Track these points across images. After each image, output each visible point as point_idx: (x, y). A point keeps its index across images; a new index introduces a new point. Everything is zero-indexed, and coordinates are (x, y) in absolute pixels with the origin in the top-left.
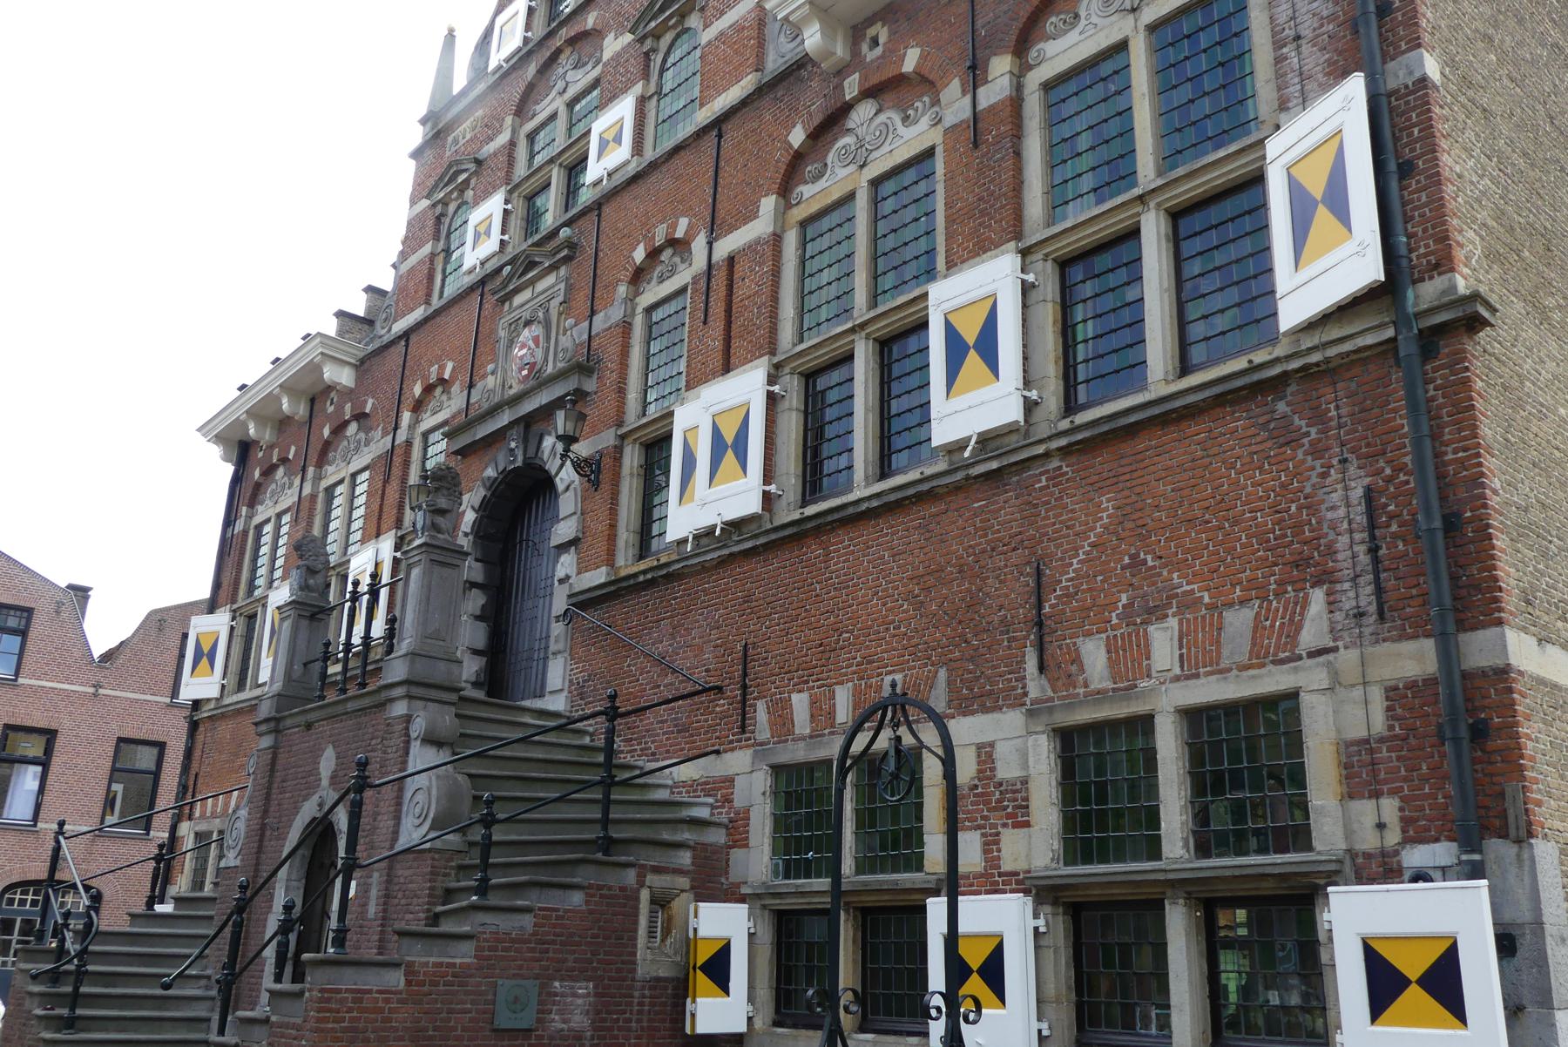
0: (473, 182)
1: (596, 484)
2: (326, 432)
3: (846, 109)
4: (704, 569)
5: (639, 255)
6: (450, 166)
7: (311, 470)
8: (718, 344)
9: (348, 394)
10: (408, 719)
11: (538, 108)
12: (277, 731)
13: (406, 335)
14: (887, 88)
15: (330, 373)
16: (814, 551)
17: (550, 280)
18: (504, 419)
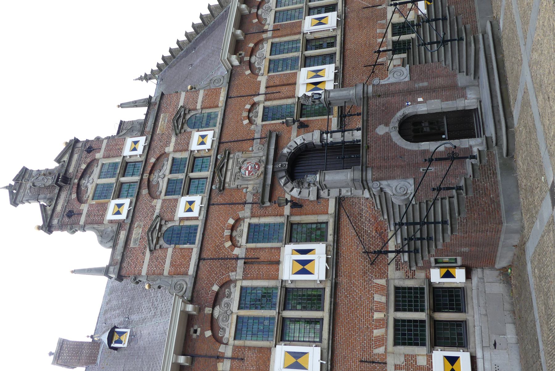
0: (163, 222)
1: (307, 126)
2: (208, 333)
3: (250, 61)
4: (343, 82)
5: (246, 122)
6: (148, 234)
7: (222, 349)
8: (287, 87)
9: (200, 310)
10: (374, 85)
11: (160, 190)
12: (366, 167)
13: (200, 259)
14: (252, 52)
15: (190, 308)
16: (348, 53)
17: (231, 161)
18: (270, 167)
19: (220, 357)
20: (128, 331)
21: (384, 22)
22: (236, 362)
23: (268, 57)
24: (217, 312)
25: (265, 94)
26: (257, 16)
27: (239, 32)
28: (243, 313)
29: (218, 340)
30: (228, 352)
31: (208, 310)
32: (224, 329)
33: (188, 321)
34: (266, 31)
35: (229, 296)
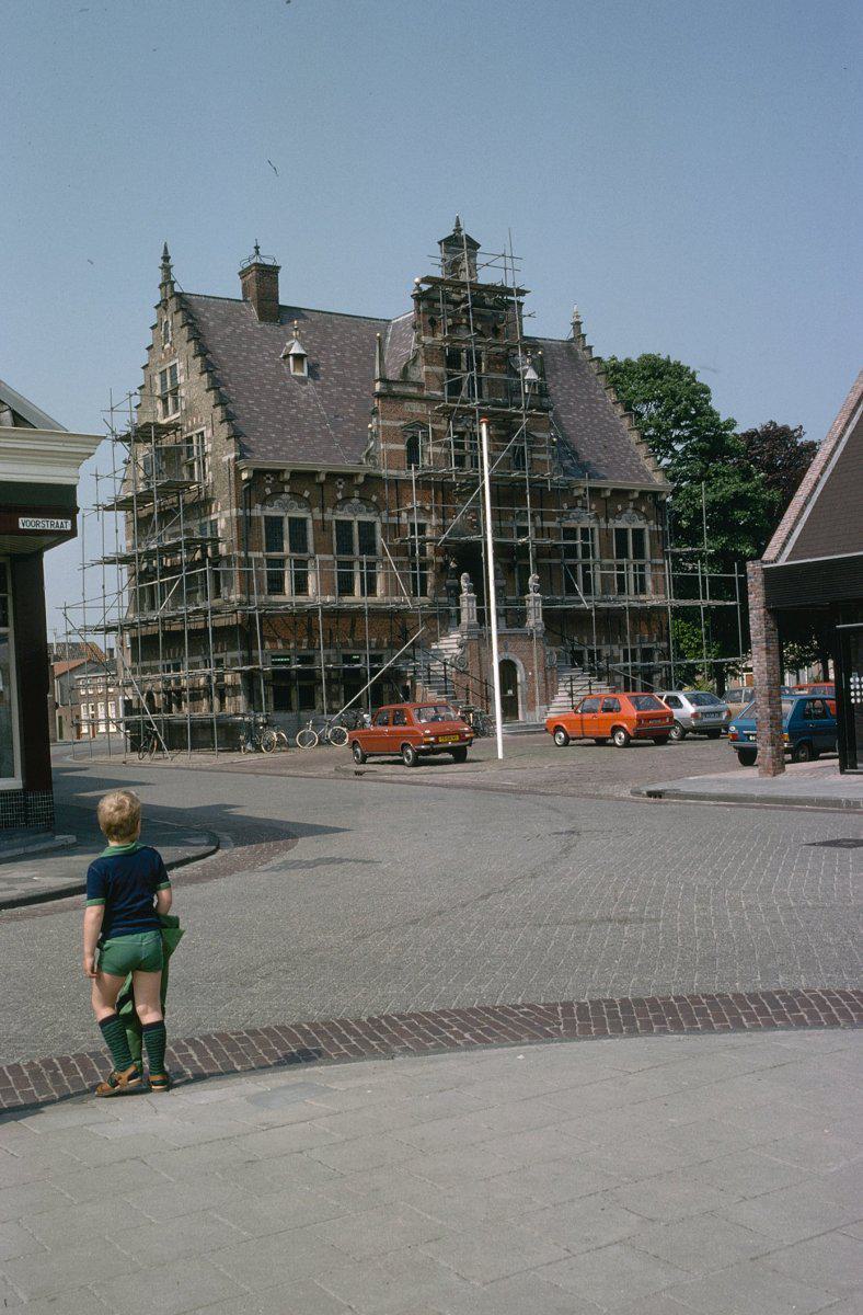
2: (340, 496)
7: (329, 510)
19: (323, 510)
20: (305, 374)
21: (603, 642)
22: (320, 525)
23: (581, 525)
24: (355, 501)
25: (542, 528)
26: (625, 509)
27: (608, 494)
28: (356, 525)
29: (336, 504)
30: (328, 517)
31: (356, 493)
32: (342, 510)
33: (349, 477)
34: (607, 522)
35: (368, 511)
